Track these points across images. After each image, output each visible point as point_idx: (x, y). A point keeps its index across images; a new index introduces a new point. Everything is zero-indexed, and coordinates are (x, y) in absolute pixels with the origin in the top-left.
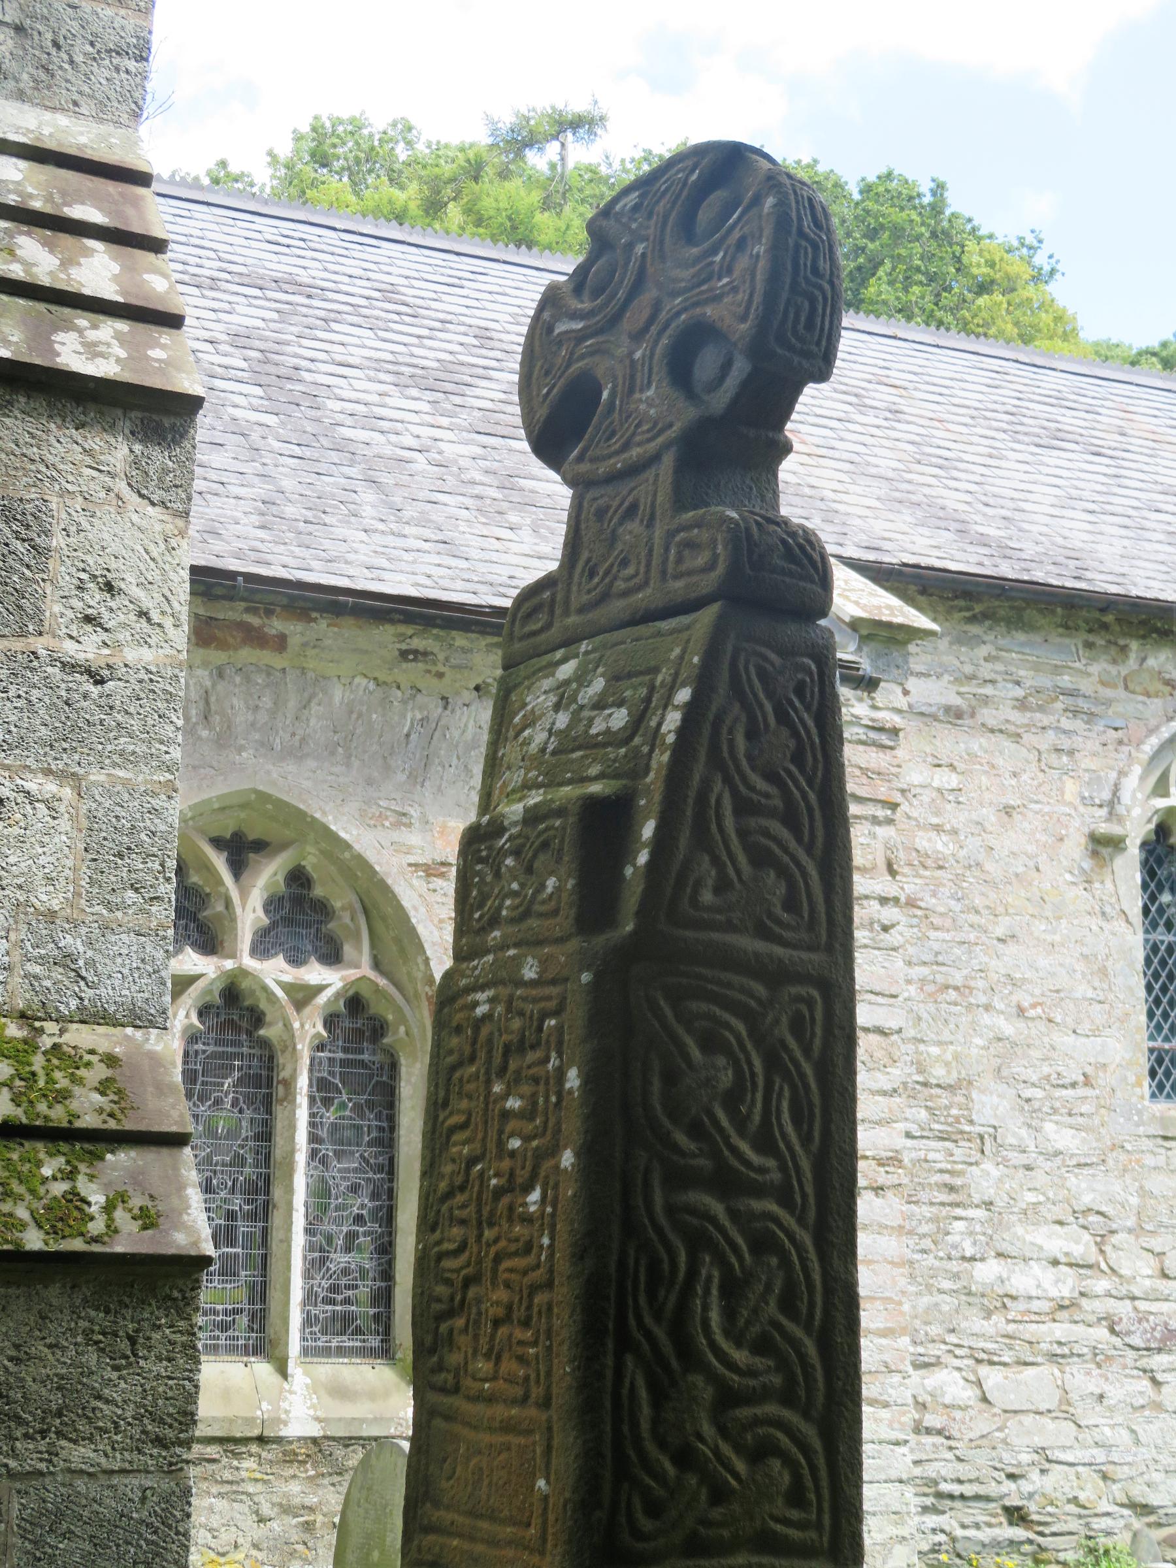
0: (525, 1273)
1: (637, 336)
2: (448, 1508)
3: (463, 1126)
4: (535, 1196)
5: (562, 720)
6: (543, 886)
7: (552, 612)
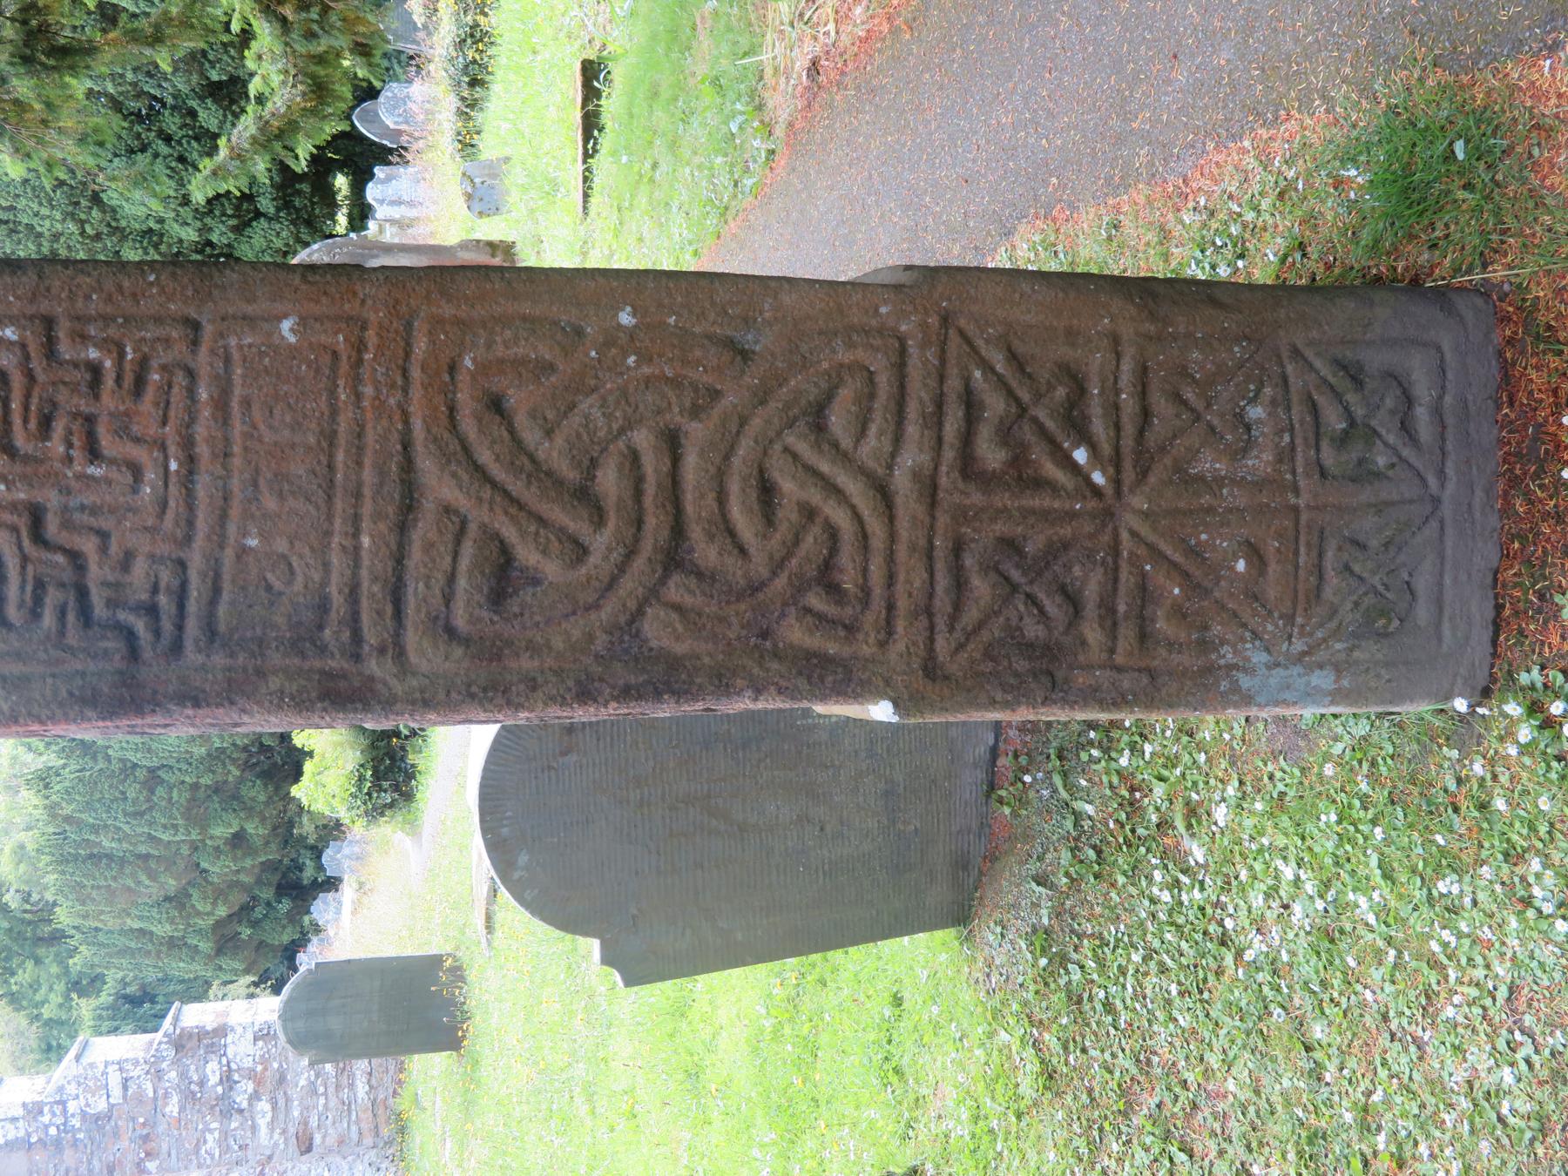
0: (30, 376)
2: (326, 566)
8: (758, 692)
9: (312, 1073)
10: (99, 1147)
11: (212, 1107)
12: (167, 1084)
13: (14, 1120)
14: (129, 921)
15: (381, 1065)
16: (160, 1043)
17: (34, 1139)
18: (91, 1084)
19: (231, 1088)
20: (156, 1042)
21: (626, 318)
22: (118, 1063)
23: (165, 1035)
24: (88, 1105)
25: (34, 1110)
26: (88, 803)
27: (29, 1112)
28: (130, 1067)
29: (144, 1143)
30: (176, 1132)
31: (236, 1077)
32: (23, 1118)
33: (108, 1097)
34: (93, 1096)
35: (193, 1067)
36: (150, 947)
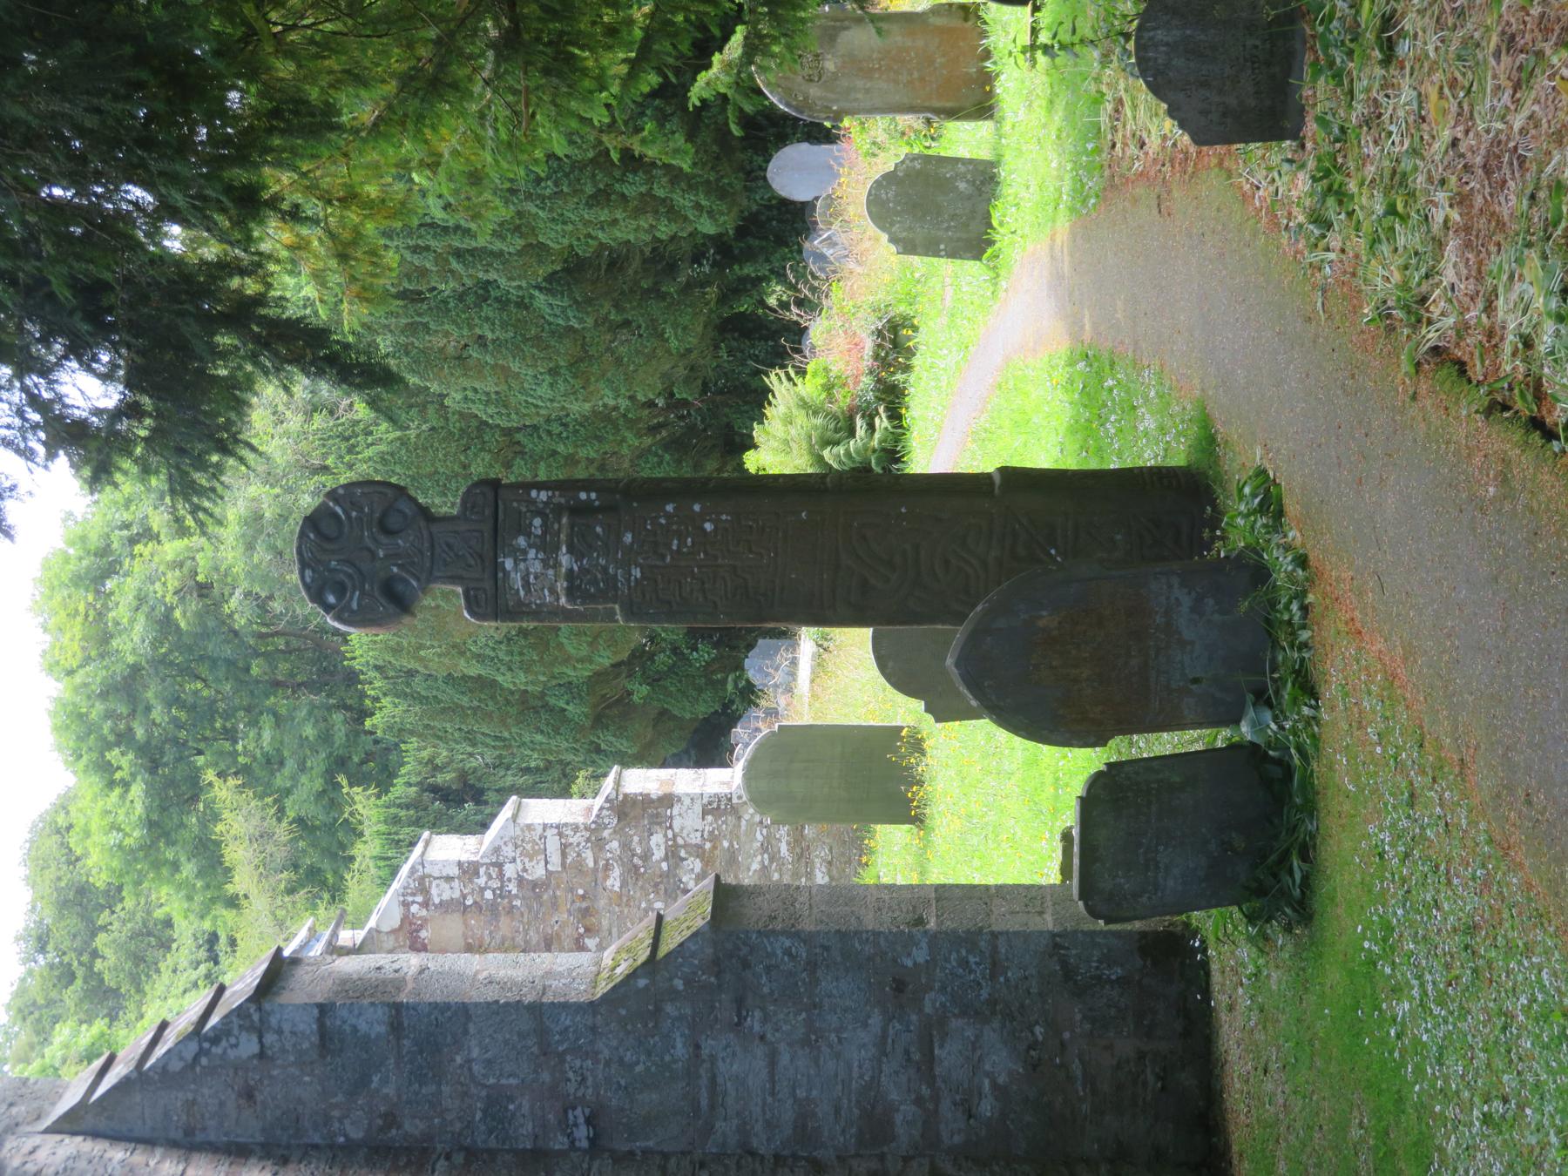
1: (373, 555)
3: (680, 587)
4: (708, 526)
5: (532, 553)
6: (598, 536)
7: (478, 589)
8: (943, 624)
9: (766, 856)
10: (536, 917)
11: (656, 885)
12: (609, 855)
13: (449, 879)
14: (462, 662)
15: (843, 854)
16: (601, 809)
17: (469, 902)
18: (528, 847)
19: (677, 866)
20: (595, 812)
21: (903, 510)
22: (558, 827)
23: (607, 800)
24: (525, 870)
25: (469, 870)
26: (413, 478)
27: (464, 872)
28: (569, 832)
29: (584, 917)
30: (617, 909)
31: (683, 854)
32: (459, 878)
33: (547, 863)
34: (531, 860)
35: (636, 839)
36: (491, 707)
